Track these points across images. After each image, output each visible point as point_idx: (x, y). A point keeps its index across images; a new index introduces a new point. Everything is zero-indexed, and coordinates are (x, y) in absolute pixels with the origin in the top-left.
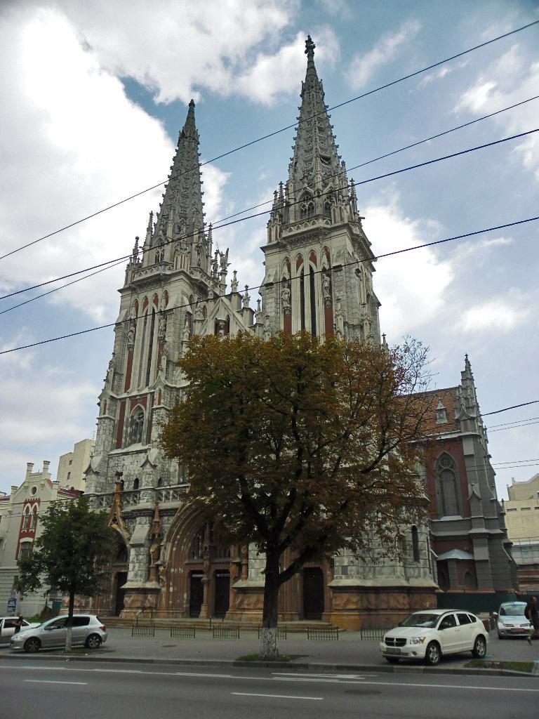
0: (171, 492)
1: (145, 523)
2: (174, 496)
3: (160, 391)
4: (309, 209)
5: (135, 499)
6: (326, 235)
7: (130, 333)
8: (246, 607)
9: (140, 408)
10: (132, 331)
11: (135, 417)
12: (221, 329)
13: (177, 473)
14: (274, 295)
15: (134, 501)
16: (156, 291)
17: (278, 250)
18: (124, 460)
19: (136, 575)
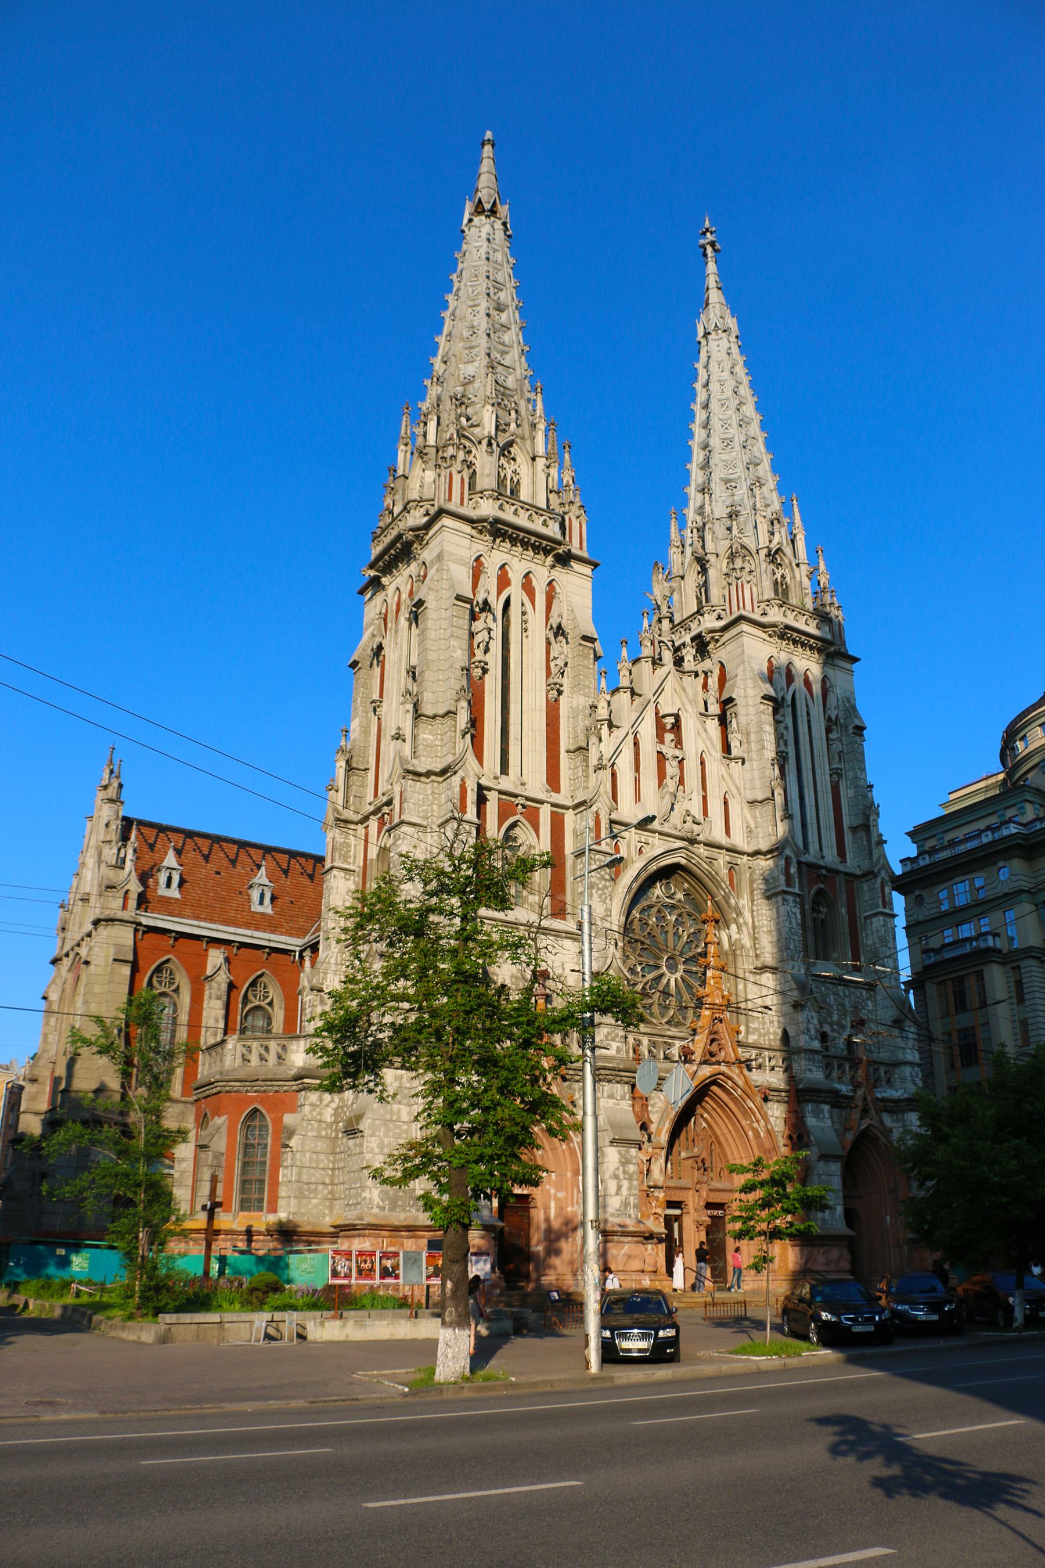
1: (623, 1098)
16: (532, 567)
19: (626, 1204)
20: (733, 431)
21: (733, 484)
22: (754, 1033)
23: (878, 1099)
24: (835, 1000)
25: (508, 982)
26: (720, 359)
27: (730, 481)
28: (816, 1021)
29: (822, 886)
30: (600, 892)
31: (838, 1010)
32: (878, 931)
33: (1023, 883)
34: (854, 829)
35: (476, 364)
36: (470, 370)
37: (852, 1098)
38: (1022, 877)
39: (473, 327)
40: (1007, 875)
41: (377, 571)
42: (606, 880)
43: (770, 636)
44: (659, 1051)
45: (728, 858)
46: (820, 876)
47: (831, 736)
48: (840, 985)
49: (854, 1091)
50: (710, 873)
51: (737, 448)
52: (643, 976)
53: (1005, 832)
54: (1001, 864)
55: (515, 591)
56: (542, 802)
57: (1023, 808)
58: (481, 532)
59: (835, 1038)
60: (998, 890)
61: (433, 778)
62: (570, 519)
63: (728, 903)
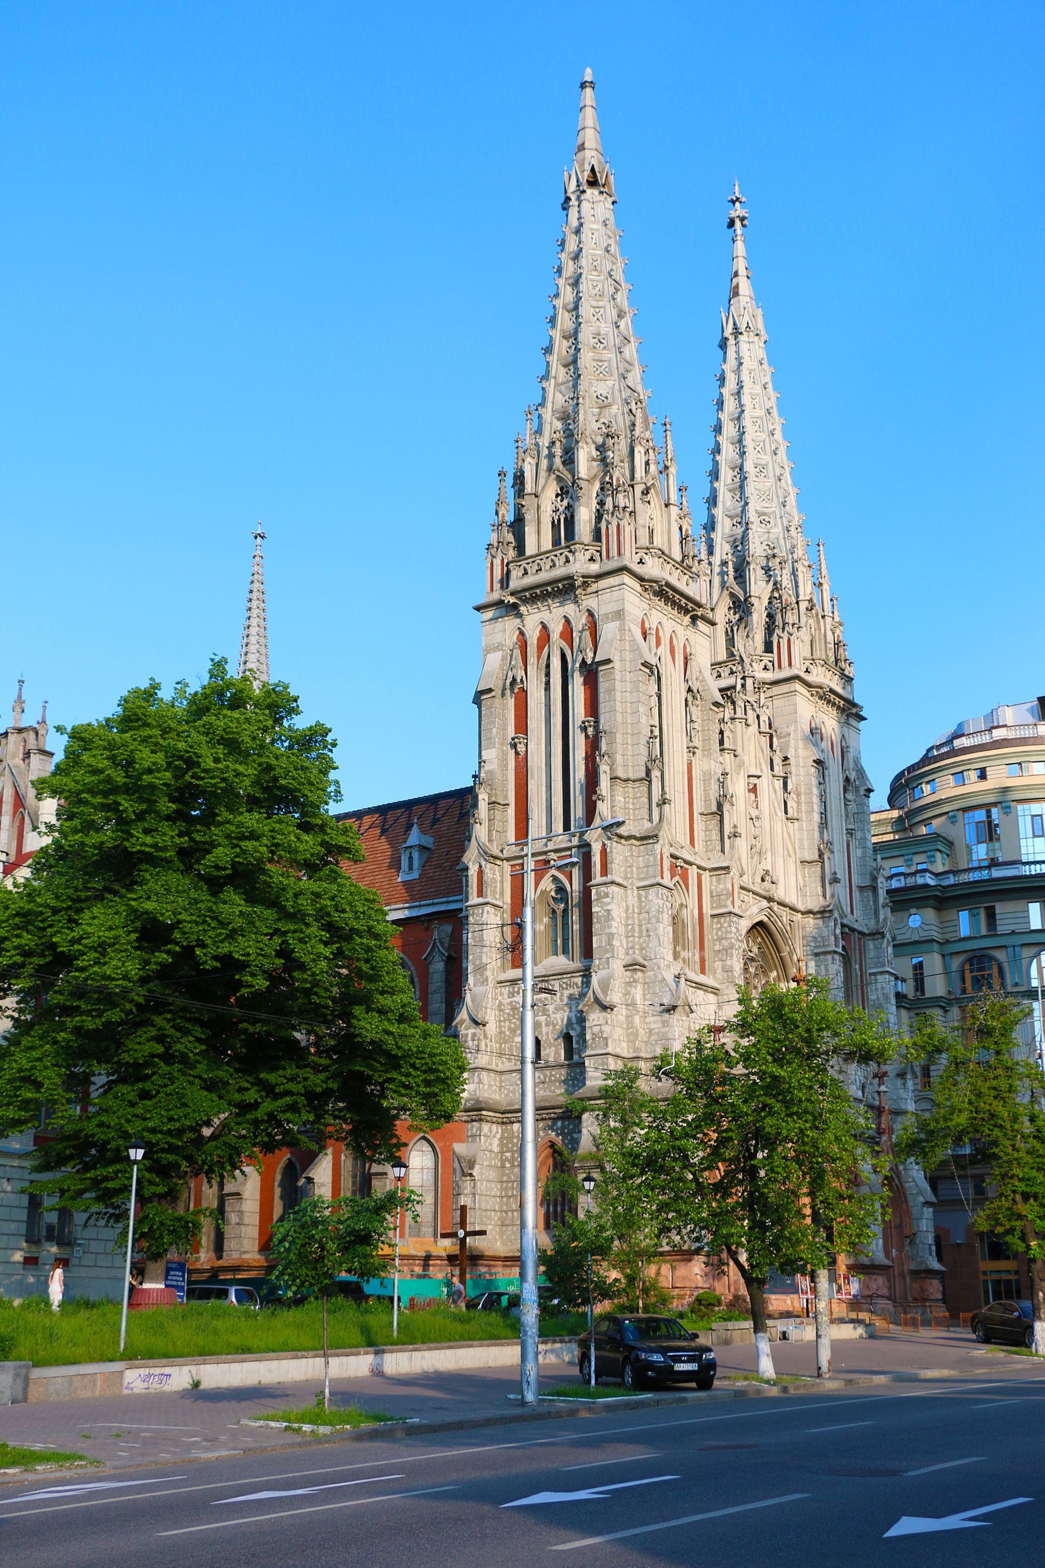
20: (766, 458)
21: (767, 519)
26: (752, 367)
27: (764, 514)
32: (883, 988)
33: (935, 934)
34: (861, 888)
35: (610, 383)
36: (602, 388)
38: (934, 928)
39: (599, 334)
40: (918, 924)
41: (520, 599)
43: (812, 695)
51: (772, 480)
53: (920, 881)
54: (913, 911)
57: (934, 856)
58: (646, 590)
60: (908, 935)
61: (633, 841)
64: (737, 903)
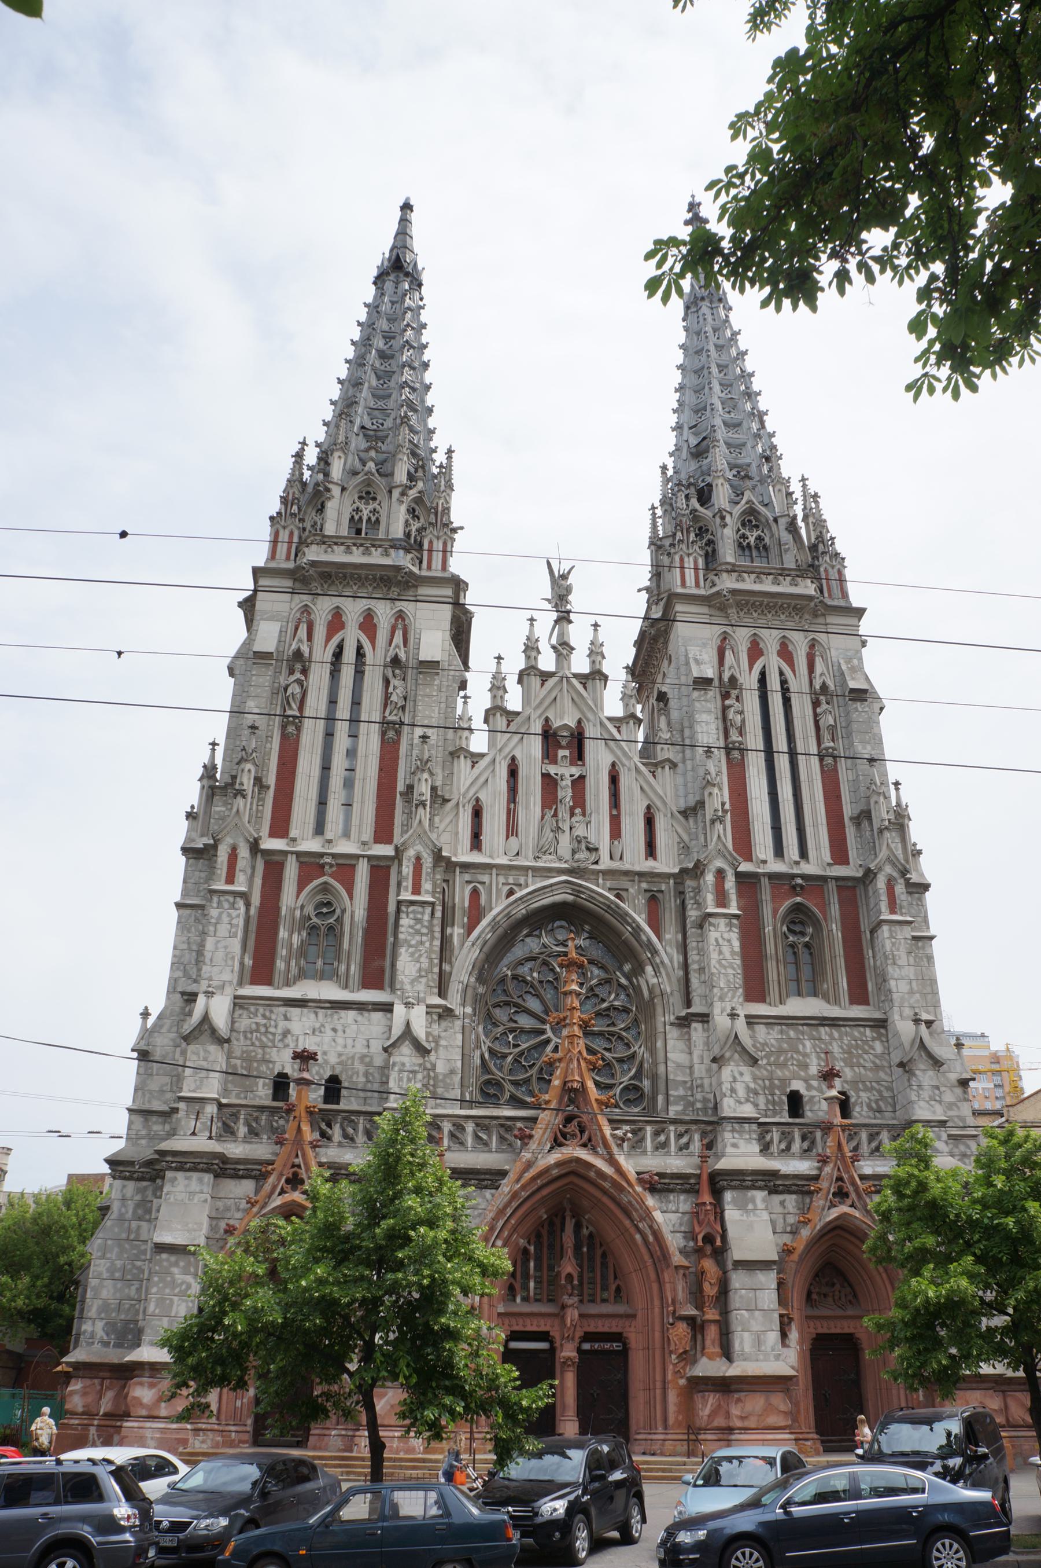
0: (470, 1127)
2: (477, 1137)
3: (418, 859)
4: (757, 548)
5: (350, 1131)
6: (816, 616)
7: (296, 689)
8: (738, 1424)
9: (325, 888)
10: (299, 682)
11: (310, 909)
12: (562, 748)
13: (457, 1079)
14: (711, 706)
15: (345, 1136)
17: (705, 610)
18: (286, 1019)
22: (676, 1104)
23: (863, 1177)
24: (814, 1046)
25: (288, 1070)
28: (747, 1078)
29: (799, 899)
30: (411, 950)
31: (819, 1058)
34: (857, 820)
37: (816, 1178)
42: (422, 934)
44: (490, 1137)
45: (644, 885)
46: (794, 887)
47: (819, 710)
48: (824, 1025)
49: (820, 1169)
50: (609, 907)
52: (516, 1046)
55: (352, 635)
56: (357, 857)
59: (813, 1097)
62: (431, 542)
63: (638, 939)
64: (427, 886)
